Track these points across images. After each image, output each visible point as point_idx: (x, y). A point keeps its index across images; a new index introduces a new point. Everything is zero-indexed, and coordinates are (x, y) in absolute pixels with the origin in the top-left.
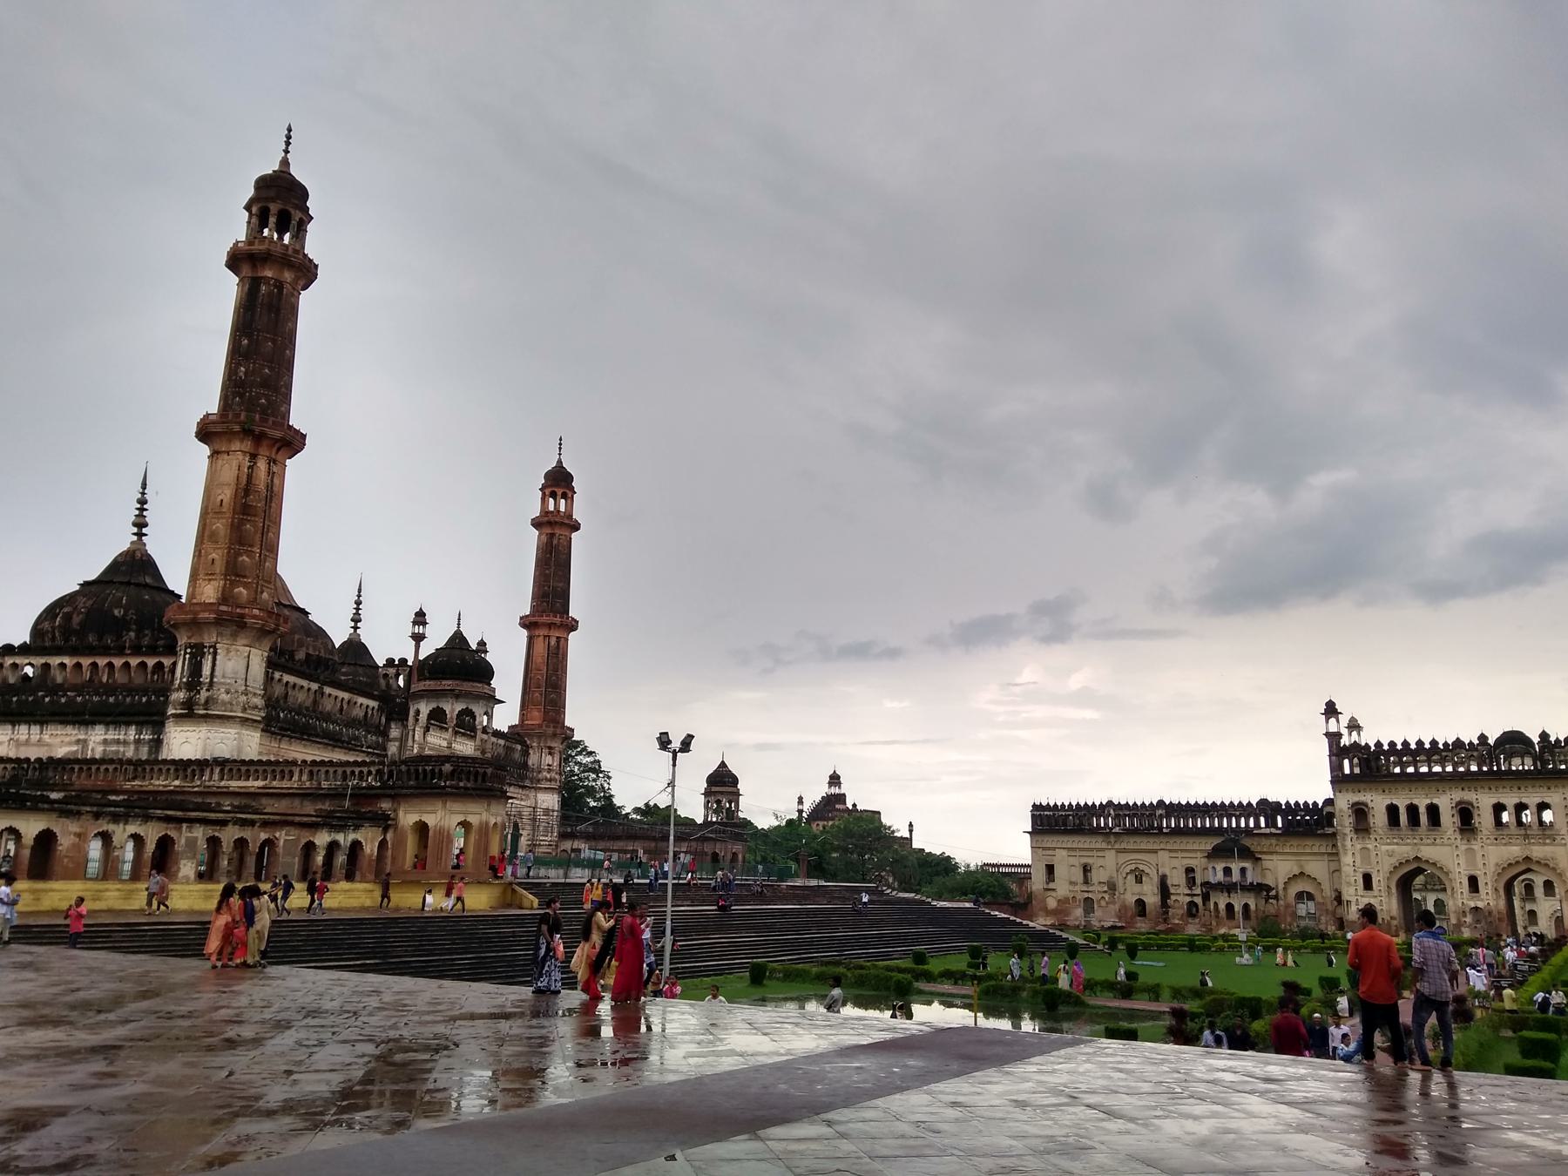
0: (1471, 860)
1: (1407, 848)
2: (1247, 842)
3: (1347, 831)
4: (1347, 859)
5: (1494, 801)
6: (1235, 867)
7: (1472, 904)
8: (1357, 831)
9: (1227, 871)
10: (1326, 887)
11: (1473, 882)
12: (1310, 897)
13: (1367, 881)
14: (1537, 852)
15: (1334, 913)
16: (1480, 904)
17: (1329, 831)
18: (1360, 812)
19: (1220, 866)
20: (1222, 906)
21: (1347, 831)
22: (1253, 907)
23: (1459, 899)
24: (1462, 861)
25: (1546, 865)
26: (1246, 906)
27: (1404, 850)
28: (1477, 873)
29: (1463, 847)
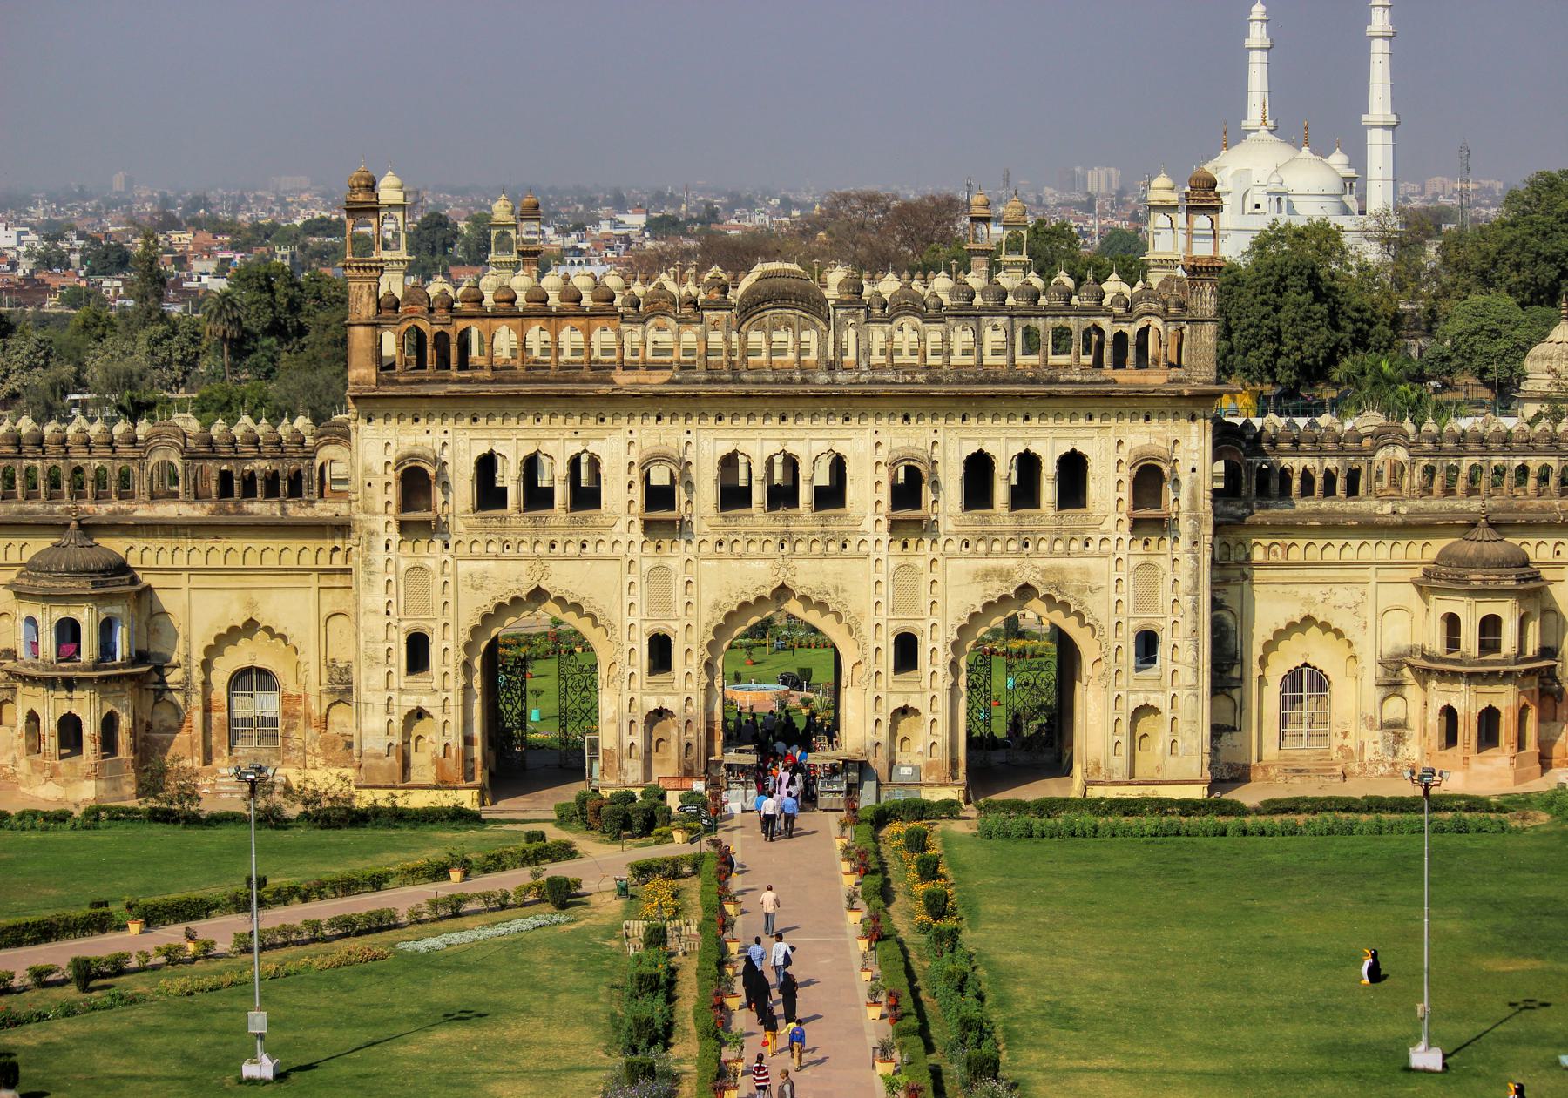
0: (661, 600)
1: (523, 567)
2: (117, 545)
3: (378, 523)
4: (375, 598)
5: (725, 448)
6: (86, 617)
7: (653, 704)
8: (403, 527)
9: (69, 632)
10: (310, 656)
11: (660, 651)
12: (264, 679)
13: (418, 652)
14: (807, 574)
15: (324, 723)
16: (671, 703)
17: (323, 510)
18: (416, 483)
19: (48, 617)
20: (49, 725)
21: (378, 523)
22: (125, 722)
23: (621, 698)
24: (639, 596)
25: (822, 606)
26: (109, 723)
27: (512, 577)
28: (674, 628)
29: (648, 564)
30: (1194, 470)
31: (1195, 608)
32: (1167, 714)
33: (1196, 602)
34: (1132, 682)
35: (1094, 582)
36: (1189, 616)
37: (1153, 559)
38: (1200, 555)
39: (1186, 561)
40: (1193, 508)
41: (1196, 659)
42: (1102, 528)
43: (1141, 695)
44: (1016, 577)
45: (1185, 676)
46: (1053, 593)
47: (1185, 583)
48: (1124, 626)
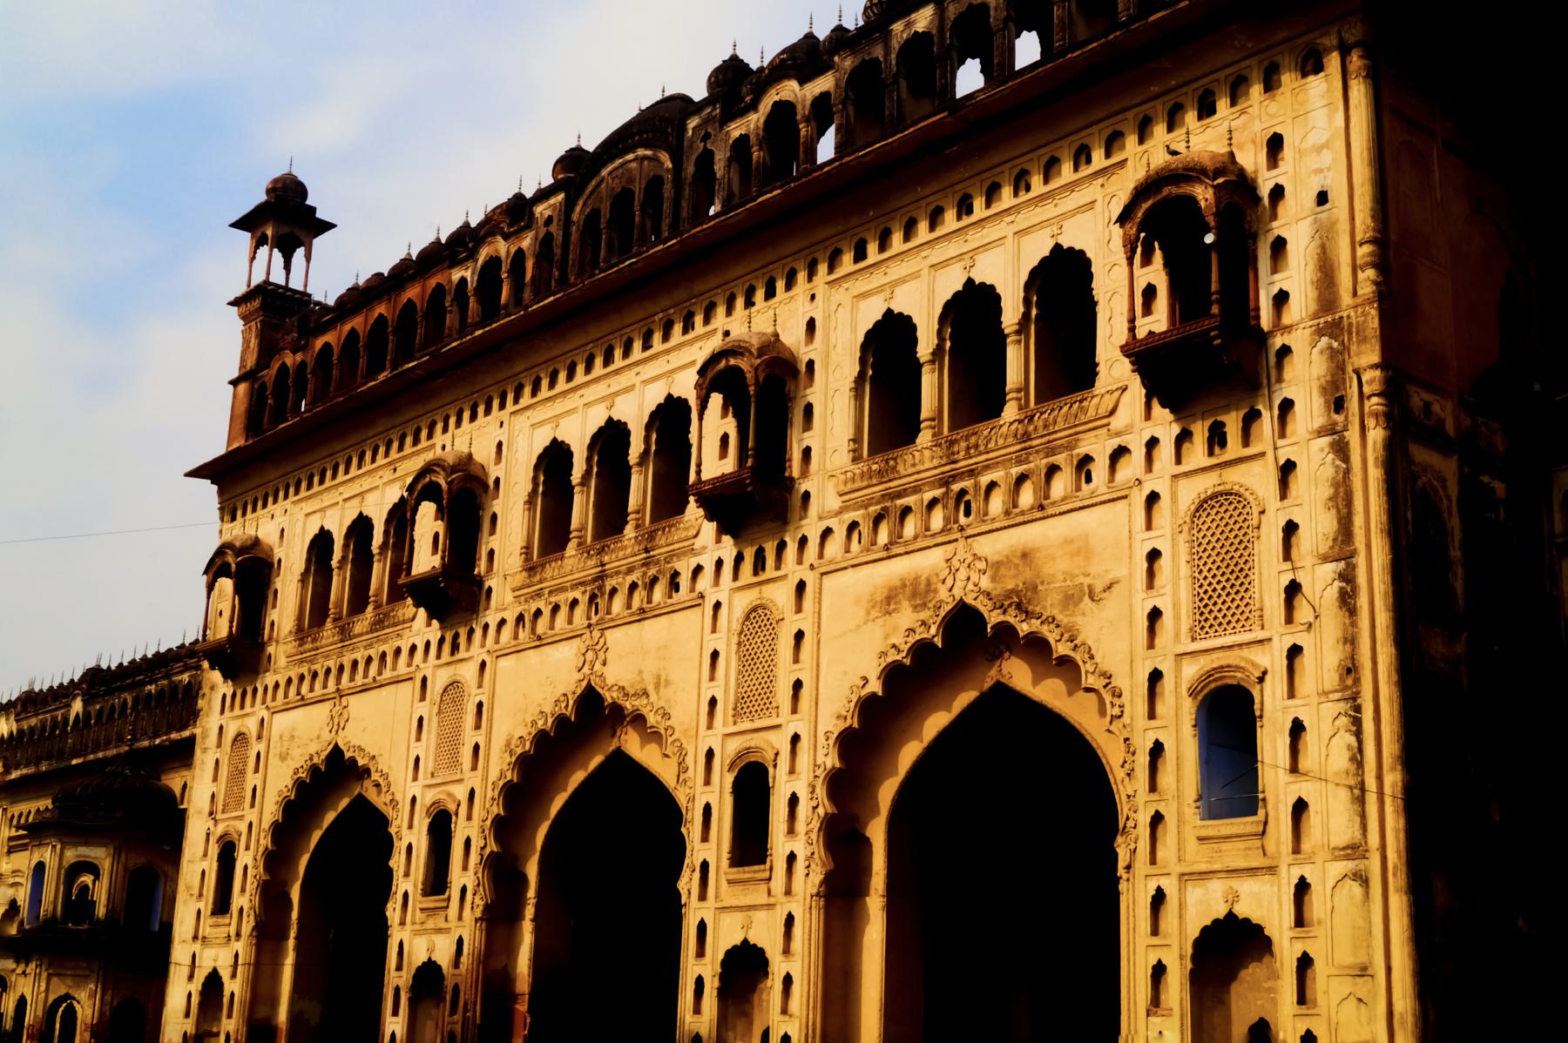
30: (1322, 198)
31: (1347, 600)
32: (1287, 949)
33: (1347, 577)
34: (1192, 845)
35: (1100, 571)
36: (1332, 623)
37: (1235, 477)
38: (1353, 436)
39: (1314, 460)
40: (1327, 299)
41: (1357, 759)
42: (1117, 422)
43: (1217, 887)
44: (943, 594)
45: (1333, 819)
46: (1010, 618)
47: (1317, 527)
48: (1168, 683)
